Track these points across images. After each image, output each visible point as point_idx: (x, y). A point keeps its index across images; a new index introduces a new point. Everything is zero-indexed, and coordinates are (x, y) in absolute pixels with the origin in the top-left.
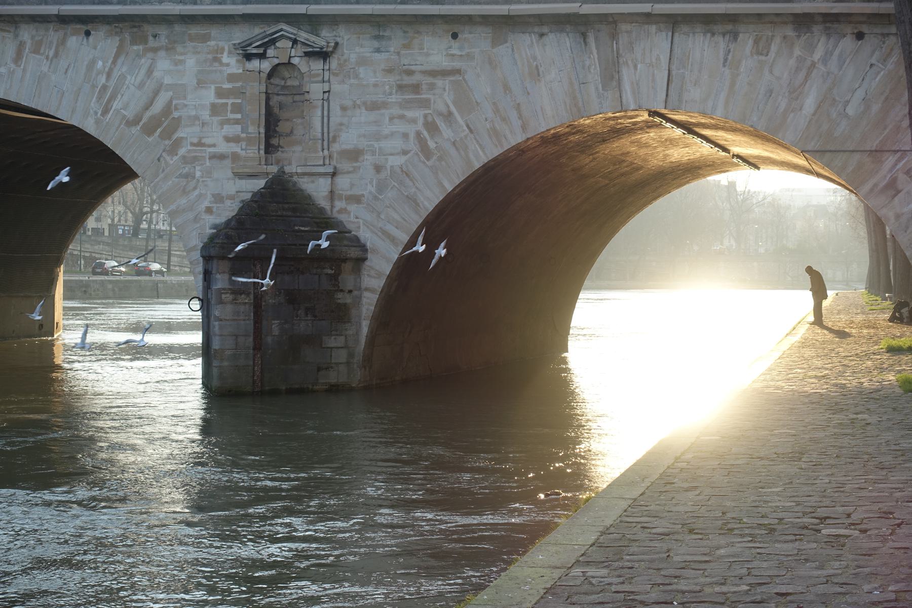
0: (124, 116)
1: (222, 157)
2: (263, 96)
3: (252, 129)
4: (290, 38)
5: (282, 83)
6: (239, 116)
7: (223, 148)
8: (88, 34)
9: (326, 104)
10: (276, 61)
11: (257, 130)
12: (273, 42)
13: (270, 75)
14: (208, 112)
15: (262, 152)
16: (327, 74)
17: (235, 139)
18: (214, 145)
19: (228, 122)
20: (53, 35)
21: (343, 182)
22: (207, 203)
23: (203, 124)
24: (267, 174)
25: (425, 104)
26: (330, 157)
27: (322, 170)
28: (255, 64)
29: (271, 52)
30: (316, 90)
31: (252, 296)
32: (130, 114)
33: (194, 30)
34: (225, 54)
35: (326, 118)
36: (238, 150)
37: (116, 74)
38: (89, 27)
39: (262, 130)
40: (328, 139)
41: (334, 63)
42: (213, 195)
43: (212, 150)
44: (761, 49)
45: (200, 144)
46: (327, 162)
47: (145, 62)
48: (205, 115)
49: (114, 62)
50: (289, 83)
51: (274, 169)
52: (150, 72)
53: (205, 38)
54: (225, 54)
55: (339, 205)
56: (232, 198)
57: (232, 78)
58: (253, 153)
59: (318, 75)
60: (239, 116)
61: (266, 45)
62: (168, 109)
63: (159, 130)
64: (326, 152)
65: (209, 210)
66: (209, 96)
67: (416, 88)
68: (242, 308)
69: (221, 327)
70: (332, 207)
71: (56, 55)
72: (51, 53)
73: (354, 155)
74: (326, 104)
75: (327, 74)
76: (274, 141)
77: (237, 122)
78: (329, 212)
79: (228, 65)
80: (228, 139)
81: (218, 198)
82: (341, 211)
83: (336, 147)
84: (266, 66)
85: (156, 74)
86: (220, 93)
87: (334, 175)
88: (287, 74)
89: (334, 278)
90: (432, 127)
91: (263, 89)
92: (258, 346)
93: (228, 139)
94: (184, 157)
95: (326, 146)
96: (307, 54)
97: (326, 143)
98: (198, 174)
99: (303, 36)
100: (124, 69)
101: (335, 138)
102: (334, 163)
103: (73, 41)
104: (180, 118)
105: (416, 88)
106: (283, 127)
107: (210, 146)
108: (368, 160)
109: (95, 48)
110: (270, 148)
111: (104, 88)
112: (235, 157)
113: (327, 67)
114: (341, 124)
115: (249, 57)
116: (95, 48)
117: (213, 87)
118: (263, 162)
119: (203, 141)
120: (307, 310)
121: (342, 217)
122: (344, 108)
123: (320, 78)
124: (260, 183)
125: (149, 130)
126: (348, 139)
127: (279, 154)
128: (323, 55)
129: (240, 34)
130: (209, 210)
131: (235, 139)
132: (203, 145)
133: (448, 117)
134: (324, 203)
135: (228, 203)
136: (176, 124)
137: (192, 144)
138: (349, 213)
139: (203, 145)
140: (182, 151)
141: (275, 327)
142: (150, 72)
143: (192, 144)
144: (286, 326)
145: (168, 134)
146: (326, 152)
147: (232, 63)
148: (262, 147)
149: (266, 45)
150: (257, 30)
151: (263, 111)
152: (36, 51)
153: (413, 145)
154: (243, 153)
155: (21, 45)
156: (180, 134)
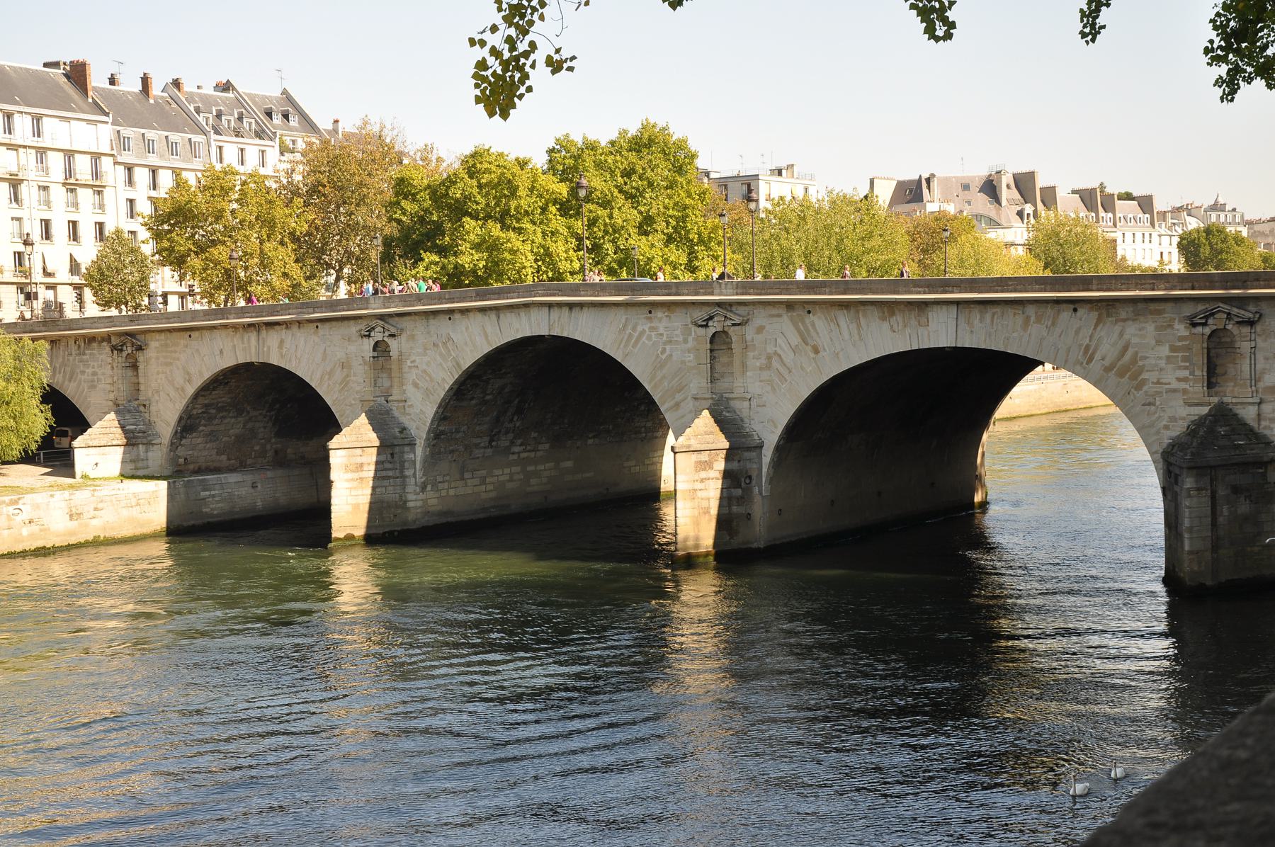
0: (1104, 365)
1: (1175, 391)
2: (1205, 351)
3: (1198, 373)
4: (1225, 312)
5: (1218, 340)
6: (1188, 364)
7: (1175, 385)
8: (1075, 310)
9: (1253, 356)
10: (1215, 327)
11: (1201, 373)
12: (1213, 314)
13: (1210, 337)
14: (1164, 361)
15: (1205, 388)
16: (1253, 335)
17: (1185, 380)
18: (1169, 384)
19: (1180, 368)
21: (1266, 408)
22: (1164, 423)
23: (1161, 370)
24: (1210, 404)
26: (1257, 391)
27: (1251, 400)
28: (1199, 329)
29: (1210, 321)
30: (1245, 346)
31: (1209, 491)
32: (1107, 363)
33: (1152, 306)
34: (1177, 321)
35: (1253, 365)
36: (1188, 387)
37: (1096, 337)
38: (1076, 306)
39: (1205, 374)
40: (1255, 379)
41: (1259, 328)
42: (1170, 417)
43: (1167, 386)
45: (1158, 383)
46: (1255, 395)
48: (1162, 363)
49: (1095, 329)
50: (1223, 340)
51: (1215, 400)
52: (1121, 335)
53: (1159, 312)
54: (1177, 321)
55: (1263, 423)
56: (1183, 419)
57: (1181, 338)
58: (1198, 389)
59: (1247, 336)
60: (1188, 364)
61: (1206, 318)
62: (1134, 360)
63: (1129, 374)
64: (1253, 388)
65: (1166, 427)
66: (1165, 351)
68: (1203, 499)
69: (1190, 513)
70: (1259, 425)
71: (1053, 324)
72: (1050, 323)
74: (1253, 356)
75: (1253, 335)
76: (1213, 380)
77: (1186, 368)
78: (1257, 429)
79: (1178, 330)
80: (1179, 380)
81: (1173, 419)
82: (1265, 428)
83: (1261, 385)
84: (1207, 331)
85: (1126, 337)
86: (1173, 349)
87: (1260, 403)
88: (1222, 335)
89: (1264, 475)
91: (1205, 345)
92: (1214, 524)
93: (1179, 380)
94: (1146, 392)
95: (1253, 384)
96: (1238, 323)
97: (1253, 382)
98: (1158, 403)
99: (1235, 311)
100: (1102, 334)
101: (1260, 378)
102: (1260, 395)
104: (1144, 365)
106: (1219, 370)
107: (1166, 384)
109: (1081, 320)
110: (1210, 385)
111: (1088, 347)
112: (1185, 391)
113: (1253, 331)
114: (1264, 369)
115: (1194, 325)
116: (1081, 320)
117: (1167, 345)
118: (1206, 395)
119: (1161, 381)
120: (1246, 497)
121: (1267, 432)
122: (1267, 359)
123: (1248, 338)
124: (1205, 410)
125: (1121, 374)
127: (1217, 389)
128: (1251, 323)
129: (1188, 310)
130: (1166, 427)
131: (1185, 380)
132: (1162, 384)
134: (1254, 424)
135: (1181, 422)
136: (1141, 370)
137: (1153, 383)
138: (1272, 429)
139: (1162, 384)
140: (1145, 388)
141: (1225, 511)
142: (1121, 335)
143: (1153, 383)
144: (1233, 509)
145: (1134, 377)
146: (1253, 388)
147: (1181, 329)
148: (1205, 385)
149: (1206, 318)
150: (1200, 307)
151: (1205, 361)
152: (1039, 320)
154: (1191, 389)
155: (1028, 318)
156: (1144, 376)
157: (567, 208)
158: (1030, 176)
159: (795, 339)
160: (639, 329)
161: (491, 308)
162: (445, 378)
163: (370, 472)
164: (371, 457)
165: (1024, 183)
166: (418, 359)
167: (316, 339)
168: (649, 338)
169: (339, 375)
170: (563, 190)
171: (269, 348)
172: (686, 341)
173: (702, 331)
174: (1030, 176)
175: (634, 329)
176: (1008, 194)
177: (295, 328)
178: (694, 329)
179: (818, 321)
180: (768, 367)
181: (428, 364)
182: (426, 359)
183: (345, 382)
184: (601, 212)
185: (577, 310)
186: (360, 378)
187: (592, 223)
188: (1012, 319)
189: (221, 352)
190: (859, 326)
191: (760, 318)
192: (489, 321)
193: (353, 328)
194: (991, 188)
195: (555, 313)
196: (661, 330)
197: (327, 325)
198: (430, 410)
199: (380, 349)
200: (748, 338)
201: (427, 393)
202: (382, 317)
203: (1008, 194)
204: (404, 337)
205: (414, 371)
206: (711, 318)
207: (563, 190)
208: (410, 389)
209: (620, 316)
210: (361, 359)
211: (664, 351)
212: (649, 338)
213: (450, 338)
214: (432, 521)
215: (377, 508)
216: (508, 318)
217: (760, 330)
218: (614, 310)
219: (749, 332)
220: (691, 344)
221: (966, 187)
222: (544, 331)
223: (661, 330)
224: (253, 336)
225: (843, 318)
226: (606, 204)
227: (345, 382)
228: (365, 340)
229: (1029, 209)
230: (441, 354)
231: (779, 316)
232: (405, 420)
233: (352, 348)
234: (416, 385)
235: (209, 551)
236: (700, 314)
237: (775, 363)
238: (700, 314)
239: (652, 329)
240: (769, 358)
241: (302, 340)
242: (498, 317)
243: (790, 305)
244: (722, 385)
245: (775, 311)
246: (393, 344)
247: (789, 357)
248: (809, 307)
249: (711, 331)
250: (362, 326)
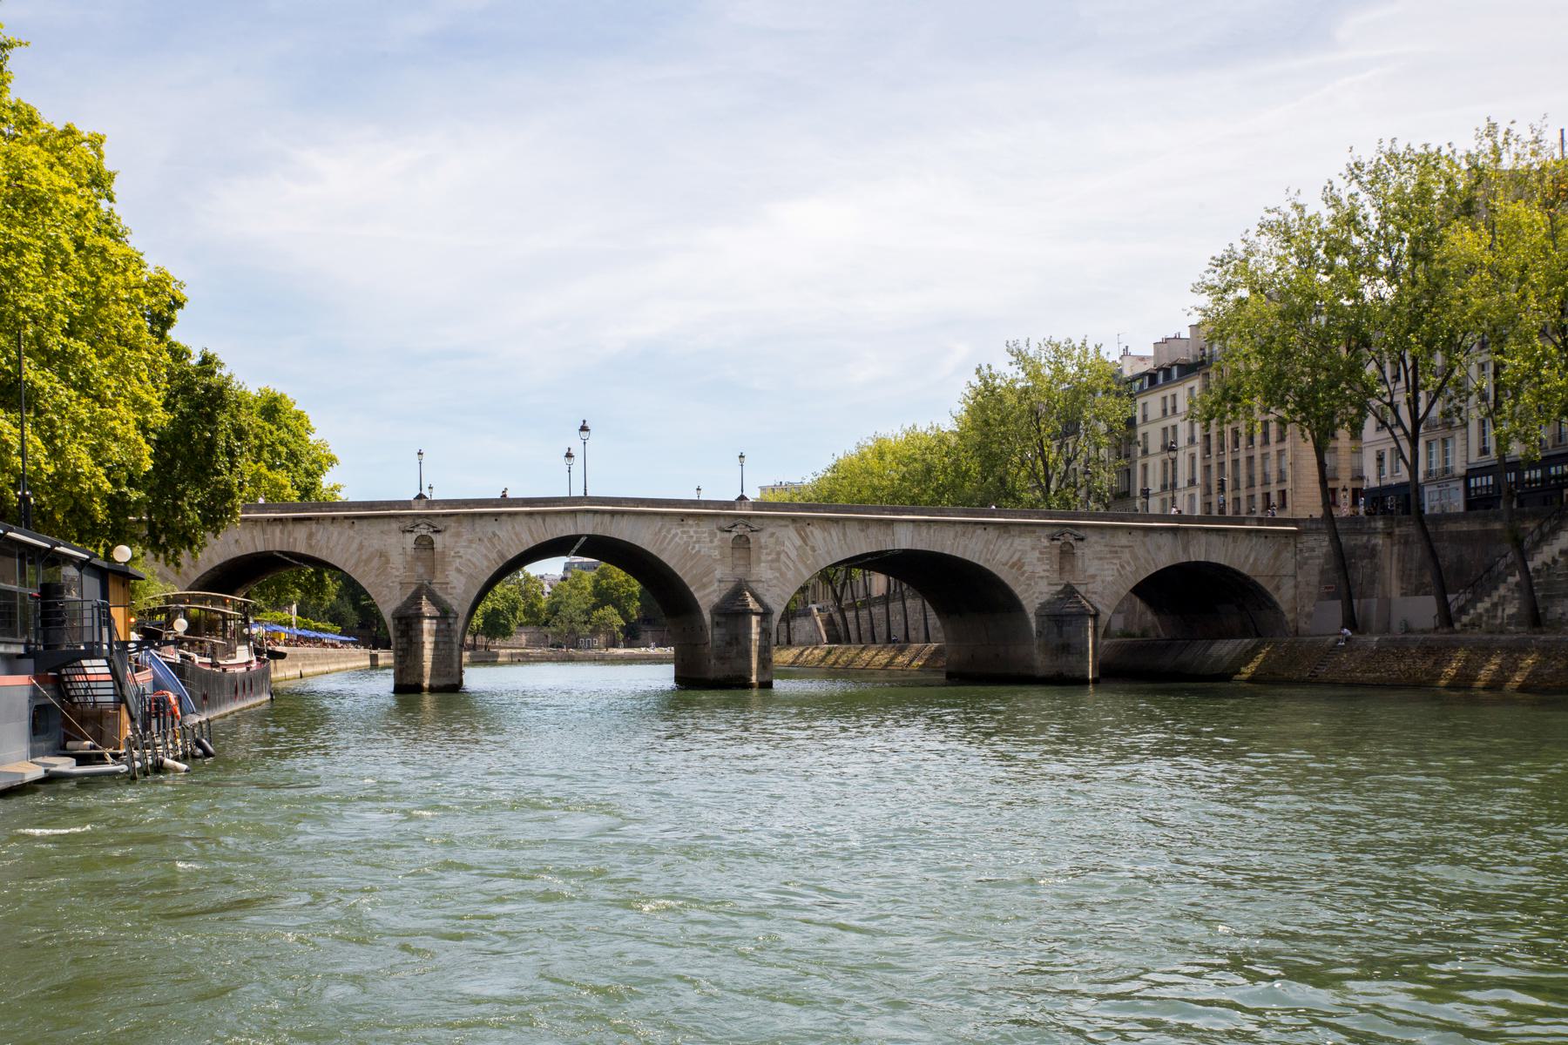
7: (1042, 574)
20: (970, 529)
21: (1090, 586)
25: (1120, 558)
30: (1078, 552)
32: (1004, 560)
33: (1030, 528)
41: (1085, 543)
44: (1235, 541)
47: (1009, 541)
48: (1035, 561)
52: (1011, 545)
62: (1019, 560)
66: (1037, 554)
67: (1116, 552)
73: (1093, 576)
81: (1041, 593)
84: (1059, 543)
86: (1041, 553)
90: (1122, 567)
99: (1076, 532)
103: (979, 532)
105: (1116, 552)
108: (1099, 578)
124: (1059, 588)
126: (1091, 571)
129: (1048, 531)
133: (1129, 563)
136: (1023, 564)
142: (1011, 545)
147: (1045, 542)
153: (1116, 573)
156: (1025, 568)
159: (798, 542)
160: (673, 532)
161: (539, 513)
166: (462, 551)
167: (352, 533)
168: (681, 538)
171: (295, 539)
172: (711, 541)
173: (726, 535)
175: (669, 531)
177: (327, 524)
178: (718, 533)
180: (777, 560)
181: (472, 555)
182: (470, 551)
185: (617, 518)
188: (950, 532)
189: (237, 541)
190: (845, 534)
193: (395, 525)
195: (598, 518)
196: (692, 533)
197: (365, 522)
199: (425, 544)
200: (763, 541)
202: (427, 516)
204: (447, 535)
205: (458, 560)
206: (735, 525)
210: (401, 551)
211: (693, 548)
212: (681, 538)
213: (494, 534)
217: (772, 535)
219: (764, 538)
220: (716, 542)
223: (692, 533)
224: (278, 529)
228: (408, 535)
230: (486, 547)
231: (786, 526)
234: (459, 571)
237: (783, 557)
238: (725, 524)
239: (684, 532)
240: (778, 554)
241: (336, 534)
242: (544, 521)
243: (794, 519)
245: (783, 523)
246: (437, 539)
248: (810, 521)
249: (734, 534)
250: (409, 523)
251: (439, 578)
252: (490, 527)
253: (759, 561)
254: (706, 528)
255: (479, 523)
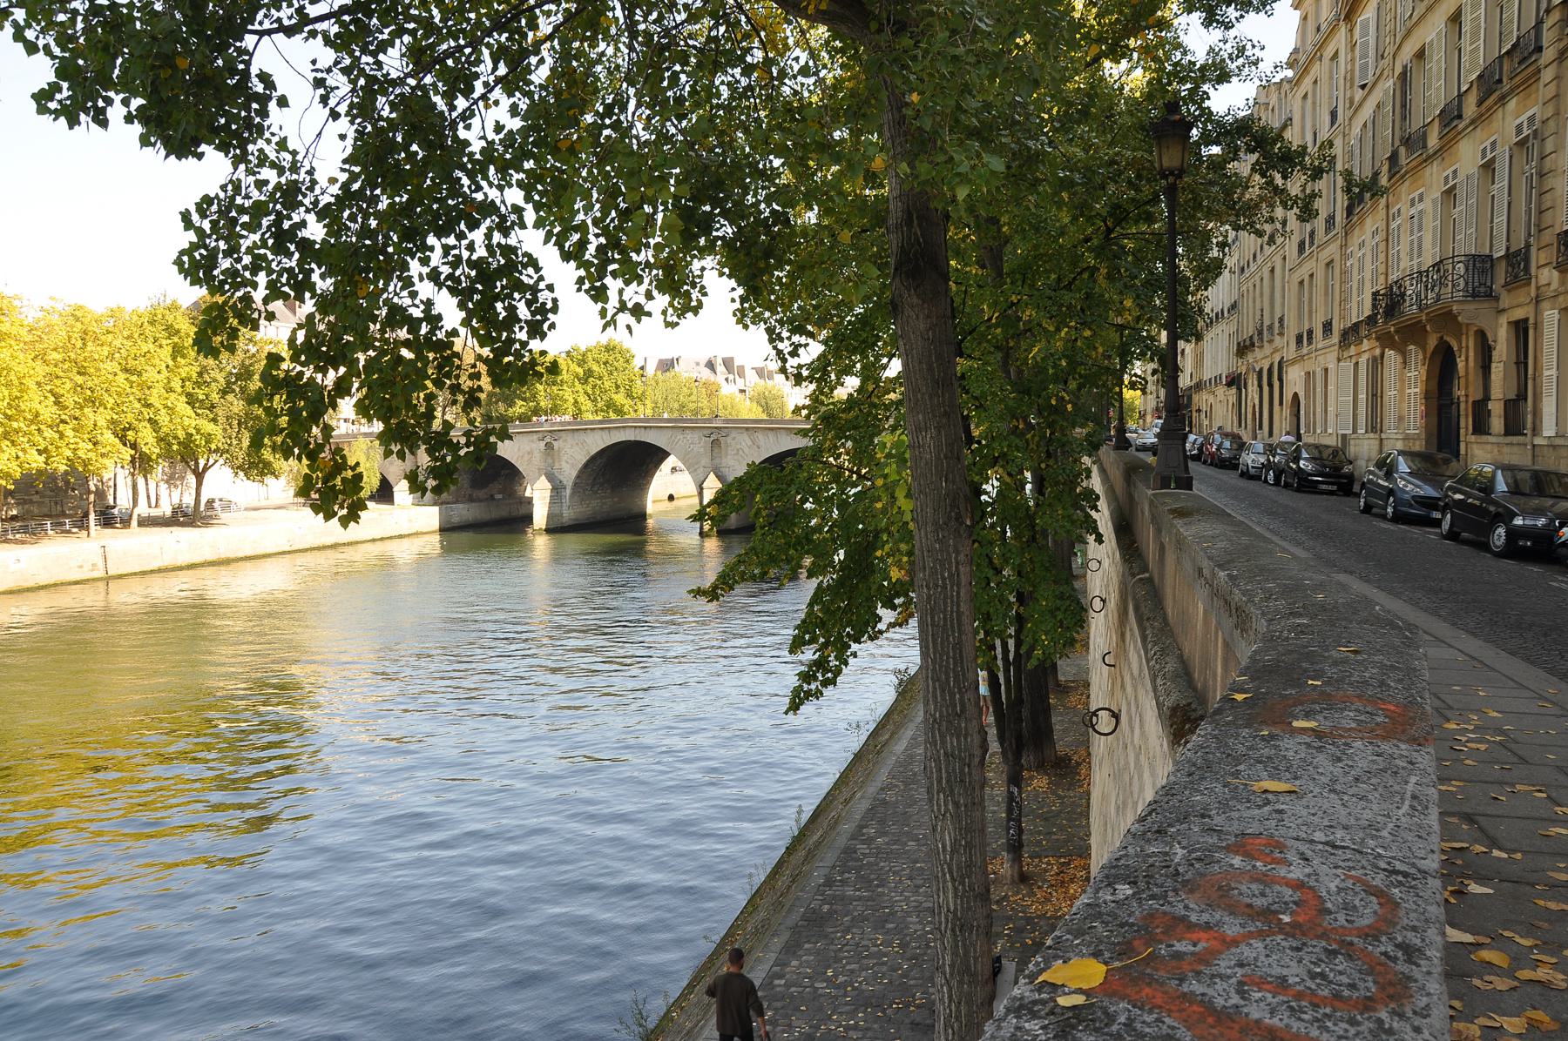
157: (584, 380)
158: (732, 359)
159: (750, 443)
162: (582, 459)
163: (548, 500)
164: (548, 493)
165: (728, 363)
169: (526, 457)
170: (580, 371)
174: (732, 359)
176: (720, 368)
179: (760, 436)
183: (530, 460)
184: (599, 382)
186: (537, 458)
187: (594, 387)
191: (734, 434)
192: (605, 434)
193: (535, 437)
194: (711, 365)
195: (638, 430)
198: (574, 473)
199: (549, 446)
201: (573, 465)
203: (720, 368)
207: (580, 371)
208: (563, 463)
209: (670, 432)
214: (571, 523)
215: (550, 516)
216: (613, 433)
218: (665, 430)
219: (729, 440)
221: (698, 364)
222: (632, 438)
225: (771, 434)
226: (600, 378)
227: (530, 460)
229: (731, 377)
232: (561, 478)
233: (534, 445)
235: (455, 536)
236: (707, 432)
238: (707, 432)
243: (747, 429)
244: (717, 461)
247: (747, 450)
250: (540, 435)
251: (557, 466)
252: (582, 436)
253: (727, 455)
254: (696, 436)
255: (576, 434)
